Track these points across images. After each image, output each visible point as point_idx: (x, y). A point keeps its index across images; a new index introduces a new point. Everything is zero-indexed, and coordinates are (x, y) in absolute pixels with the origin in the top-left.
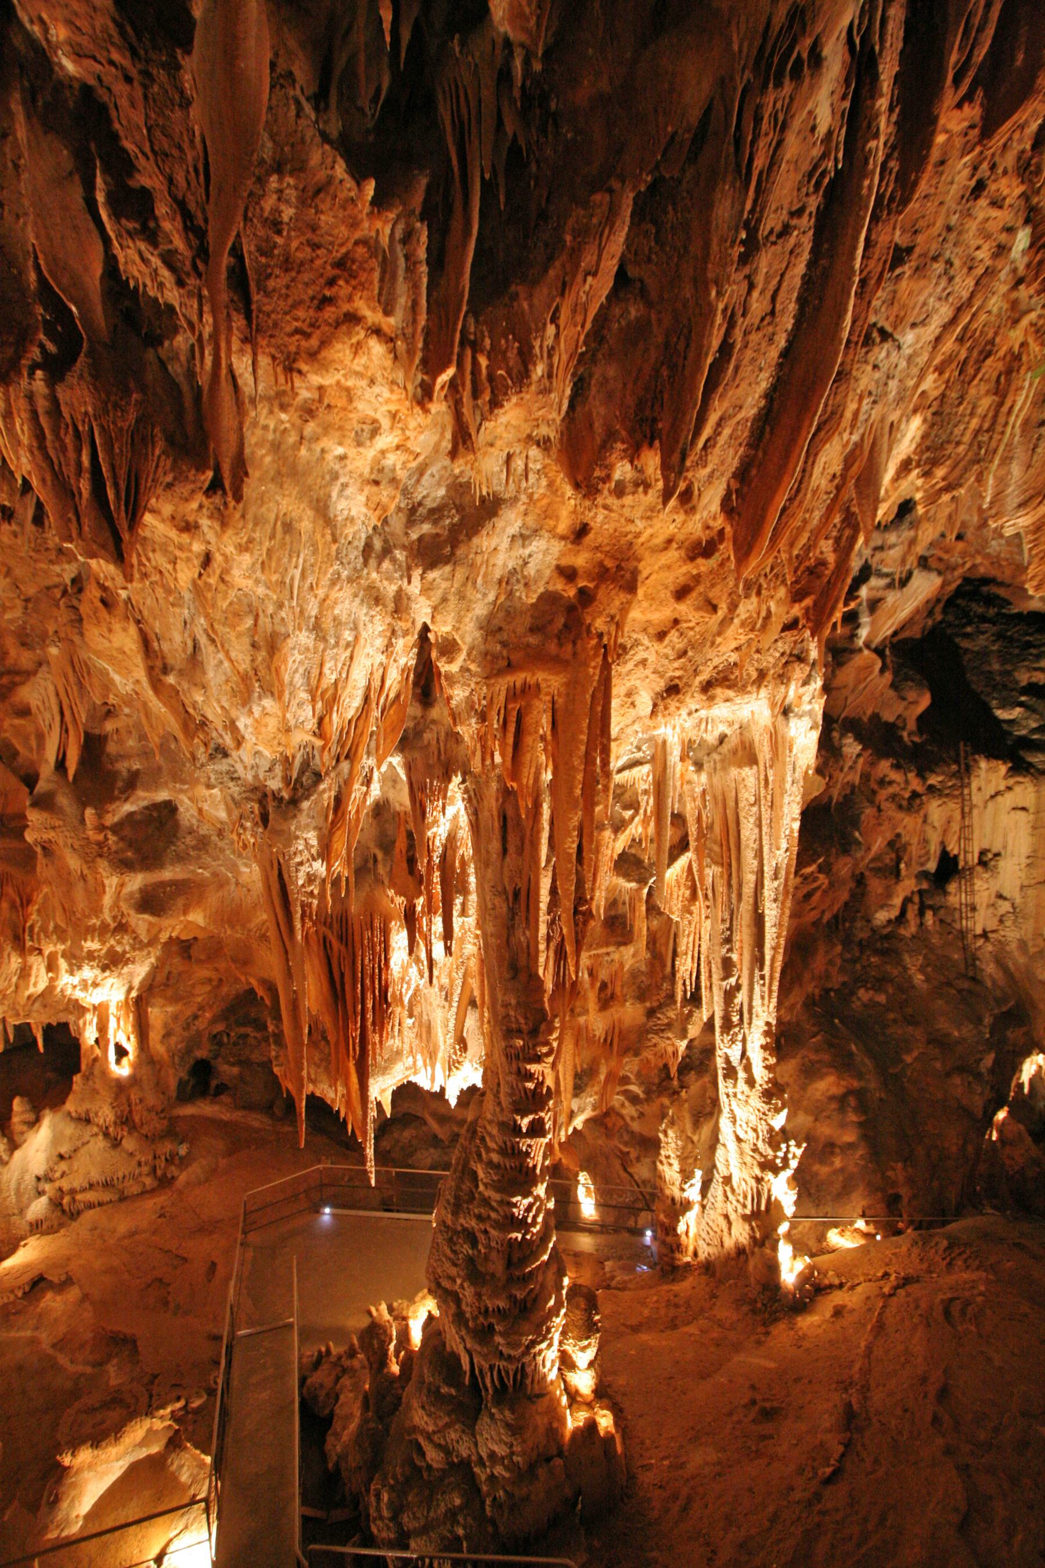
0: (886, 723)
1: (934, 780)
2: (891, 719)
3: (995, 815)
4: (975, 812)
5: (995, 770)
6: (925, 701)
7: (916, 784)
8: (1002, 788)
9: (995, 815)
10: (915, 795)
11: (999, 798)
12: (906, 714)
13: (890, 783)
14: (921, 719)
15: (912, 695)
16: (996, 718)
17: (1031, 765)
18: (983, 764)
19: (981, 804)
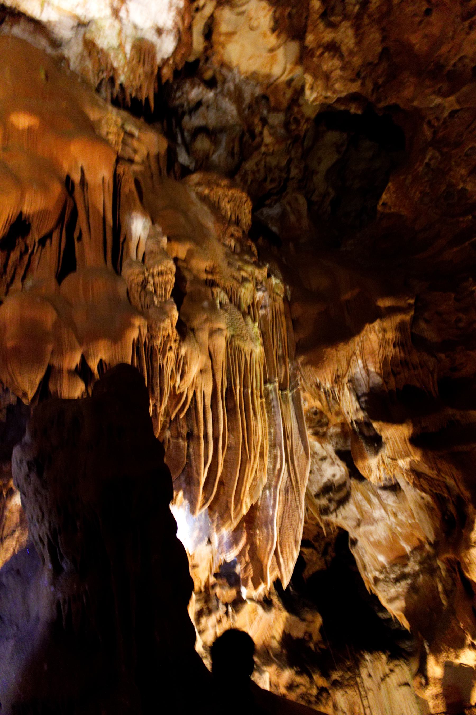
0: (298, 639)
1: (335, 676)
2: (301, 635)
3: (388, 692)
4: (370, 695)
5: (379, 659)
6: (319, 620)
7: (321, 682)
8: (387, 671)
9: (388, 692)
10: (322, 690)
11: (387, 679)
12: (310, 630)
13: (297, 686)
14: (322, 630)
15: (309, 617)
16: (379, 618)
17: (404, 650)
18: (368, 657)
19: (374, 688)
